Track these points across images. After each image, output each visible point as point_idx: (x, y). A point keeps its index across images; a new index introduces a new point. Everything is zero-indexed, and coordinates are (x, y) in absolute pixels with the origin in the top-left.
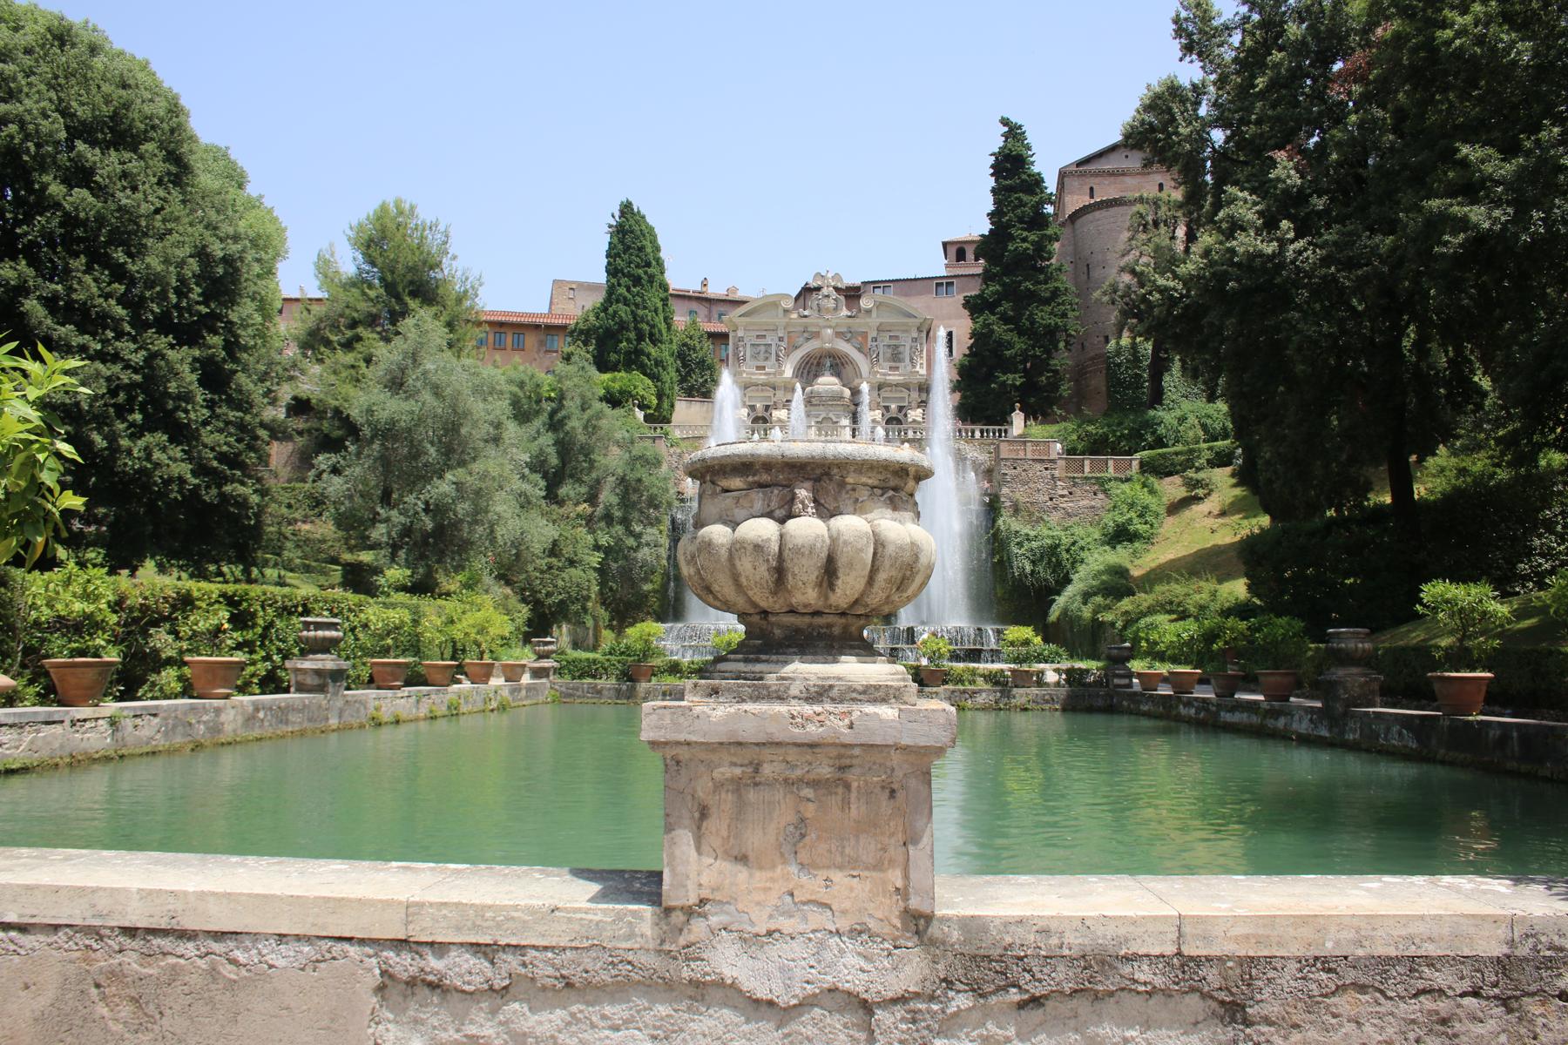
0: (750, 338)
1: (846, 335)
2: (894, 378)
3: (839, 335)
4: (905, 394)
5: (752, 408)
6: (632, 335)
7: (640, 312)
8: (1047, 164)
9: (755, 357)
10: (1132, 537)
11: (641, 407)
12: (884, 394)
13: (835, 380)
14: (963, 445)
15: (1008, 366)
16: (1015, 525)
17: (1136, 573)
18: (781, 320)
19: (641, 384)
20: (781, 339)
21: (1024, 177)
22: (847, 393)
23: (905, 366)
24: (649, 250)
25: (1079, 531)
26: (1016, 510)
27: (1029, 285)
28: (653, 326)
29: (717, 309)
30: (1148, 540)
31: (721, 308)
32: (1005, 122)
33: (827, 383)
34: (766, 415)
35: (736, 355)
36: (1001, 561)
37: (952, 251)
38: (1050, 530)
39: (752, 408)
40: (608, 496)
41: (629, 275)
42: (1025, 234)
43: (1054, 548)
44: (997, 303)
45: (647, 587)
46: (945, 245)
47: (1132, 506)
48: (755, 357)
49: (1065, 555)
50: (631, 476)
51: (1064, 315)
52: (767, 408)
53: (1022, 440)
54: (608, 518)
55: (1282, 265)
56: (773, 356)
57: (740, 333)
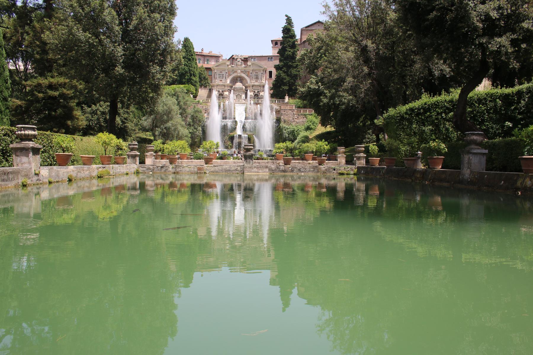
0: (218, 72)
1: (244, 72)
2: (256, 84)
3: (242, 72)
4: (259, 88)
5: (219, 91)
6: (189, 75)
9: (219, 77)
10: (311, 129)
11: (192, 94)
13: (241, 84)
14: (273, 104)
15: (285, 84)
16: (284, 125)
17: (310, 137)
19: (192, 88)
22: (244, 87)
23: (259, 81)
25: (299, 127)
26: (285, 122)
27: (290, 63)
29: (207, 58)
30: (314, 130)
31: (208, 58)
32: (286, 16)
33: (239, 85)
37: (274, 43)
38: (292, 127)
39: (219, 91)
40: (189, 120)
41: (187, 58)
43: (293, 131)
44: (282, 68)
45: (196, 140)
46: (272, 41)
47: (311, 122)
48: (219, 77)
50: (195, 115)
51: (299, 71)
52: (223, 91)
53: (287, 103)
54: (189, 125)
55: (319, 90)
57: (215, 71)
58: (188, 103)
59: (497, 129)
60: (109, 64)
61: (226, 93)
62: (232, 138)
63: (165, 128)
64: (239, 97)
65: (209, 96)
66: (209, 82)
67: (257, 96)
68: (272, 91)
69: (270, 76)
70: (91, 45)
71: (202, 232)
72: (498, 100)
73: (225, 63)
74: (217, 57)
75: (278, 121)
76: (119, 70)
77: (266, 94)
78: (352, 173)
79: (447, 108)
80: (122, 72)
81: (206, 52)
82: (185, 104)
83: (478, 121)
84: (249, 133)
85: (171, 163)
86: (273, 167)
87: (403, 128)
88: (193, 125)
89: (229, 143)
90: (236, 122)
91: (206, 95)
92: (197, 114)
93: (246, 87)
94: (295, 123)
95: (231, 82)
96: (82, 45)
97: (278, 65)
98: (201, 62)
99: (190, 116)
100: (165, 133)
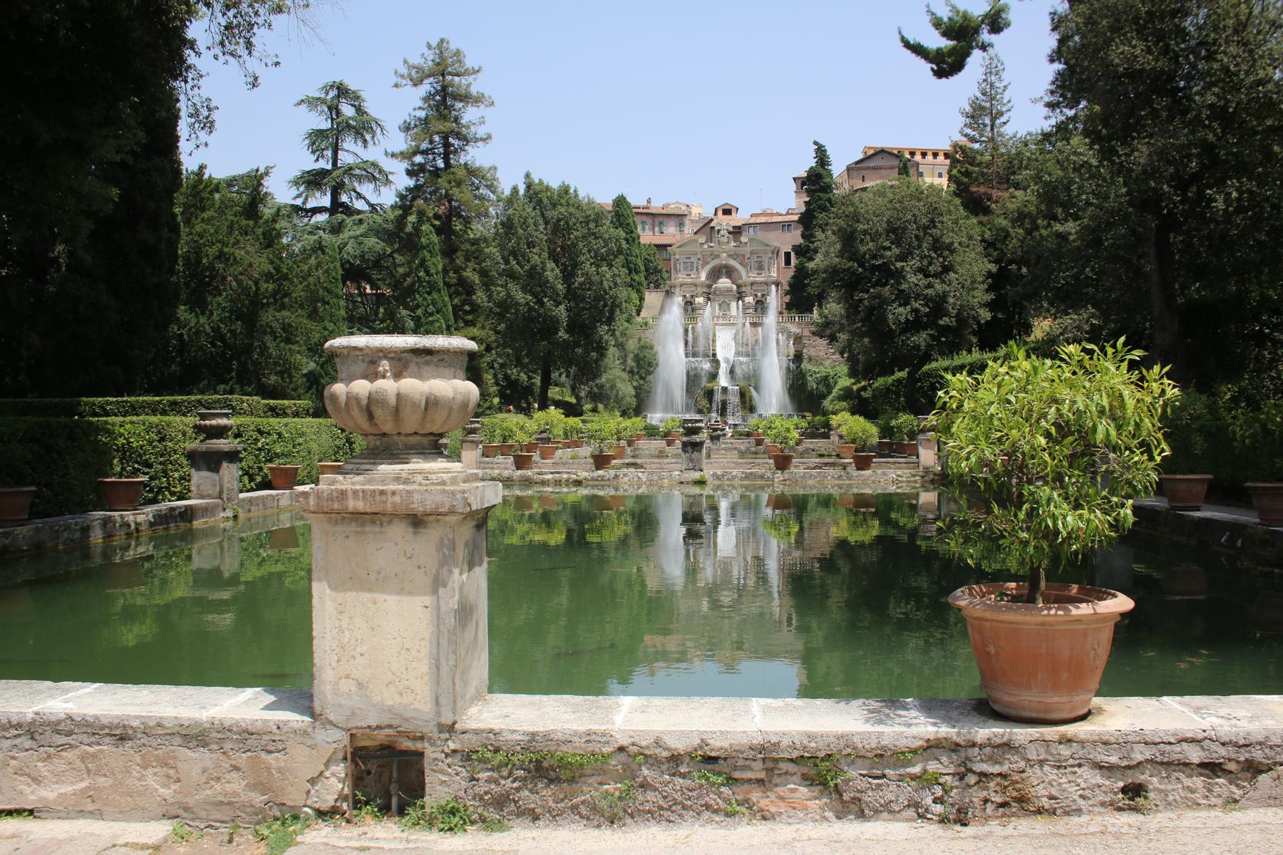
2: (759, 279)
3: (730, 256)
8: (837, 168)
9: (685, 269)
14: (789, 325)
18: (699, 249)
22: (735, 287)
25: (838, 369)
26: (810, 359)
29: (657, 220)
31: (661, 219)
32: (815, 143)
33: (724, 283)
38: (822, 371)
40: (630, 362)
43: (826, 378)
48: (685, 269)
60: (550, 326)
61: (700, 300)
62: (710, 394)
64: (724, 306)
66: (665, 275)
67: (761, 305)
68: (787, 299)
69: (788, 262)
70: (531, 309)
71: (652, 583)
73: (696, 241)
75: (798, 357)
76: (562, 334)
77: (774, 300)
82: (623, 334)
84: (742, 384)
86: (743, 448)
89: (704, 403)
90: (716, 362)
92: (646, 352)
93: (739, 286)
95: (709, 276)
97: (799, 246)
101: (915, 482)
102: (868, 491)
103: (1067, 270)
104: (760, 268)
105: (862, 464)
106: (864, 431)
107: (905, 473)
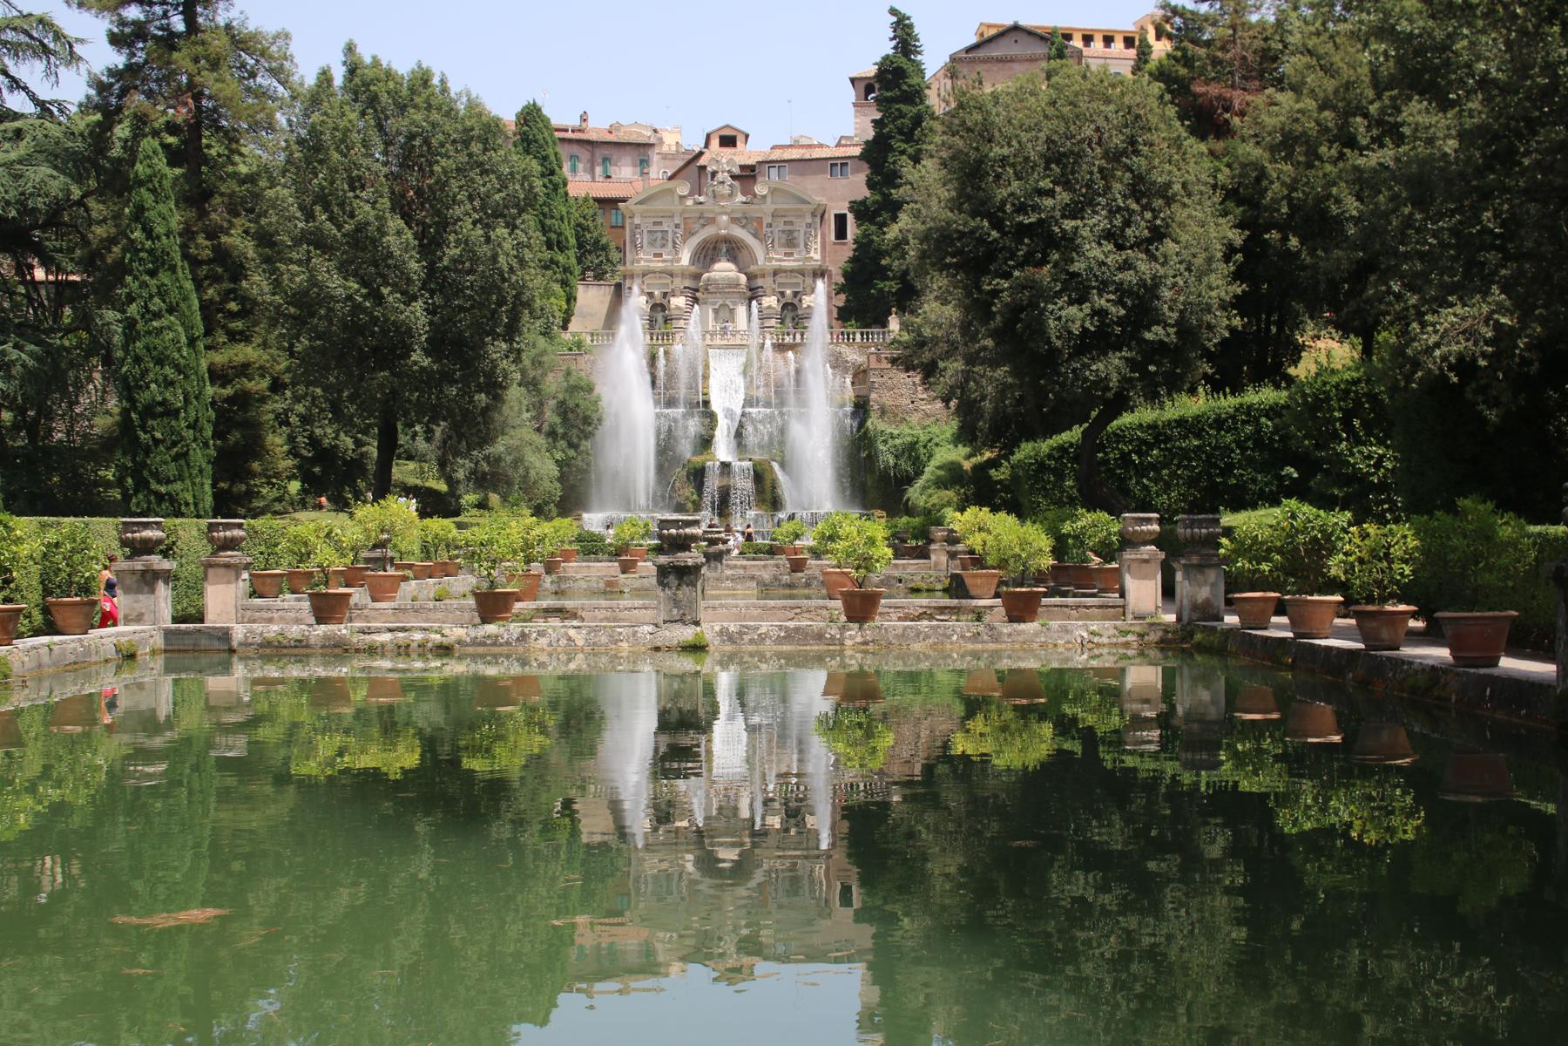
0: (647, 225)
2: (789, 264)
3: (734, 220)
4: (800, 279)
5: (651, 295)
7: (548, 222)
8: (932, 59)
9: (652, 243)
12: (779, 280)
13: (731, 266)
14: (844, 349)
16: (881, 426)
20: (677, 226)
21: (905, 87)
22: (743, 278)
24: (552, 158)
25: (935, 429)
26: (883, 412)
28: (560, 234)
29: (600, 153)
31: (606, 152)
32: (893, 11)
33: (724, 269)
34: (664, 302)
35: (633, 242)
36: (869, 456)
37: (862, 86)
38: (906, 432)
39: (651, 295)
40: (550, 417)
42: (904, 146)
43: (913, 446)
44: (877, 213)
46: (853, 80)
48: (652, 243)
49: (922, 450)
50: (571, 404)
52: (665, 295)
56: (670, 244)
57: (637, 221)
58: (545, 359)
59: (1267, 484)
60: (394, 344)
61: (679, 302)
62: (698, 476)
63: (487, 458)
64: (724, 314)
65: (612, 318)
66: (615, 256)
67: (793, 314)
68: (841, 300)
69: (841, 233)
70: (357, 308)
72: (1263, 420)
74: (640, 150)
75: (861, 408)
76: (419, 358)
78: (939, 587)
79: (1144, 442)
80: (425, 364)
81: (598, 127)
82: (536, 363)
83: (1216, 466)
84: (756, 457)
85: (548, 572)
86: (766, 576)
87: (1044, 488)
88: (564, 436)
89: (688, 491)
90: (711, 417)
91: (604, 309)
92: (579, 398)
93: (750, 277)
94: (920, 415)
95: (693, 261)
96: (338, 306)
97: (863, 202)
98: (580, 166)
99: (552, 403)
100: (484, 474)
101: (1127, 645)
102: (1031, 664)
103: (1441, 216)
104: (791, 242)
105: (1021, 609)
106: (1024, 543)
107: (1105, 628)
